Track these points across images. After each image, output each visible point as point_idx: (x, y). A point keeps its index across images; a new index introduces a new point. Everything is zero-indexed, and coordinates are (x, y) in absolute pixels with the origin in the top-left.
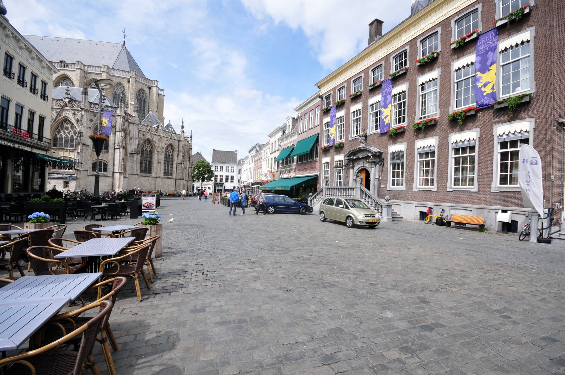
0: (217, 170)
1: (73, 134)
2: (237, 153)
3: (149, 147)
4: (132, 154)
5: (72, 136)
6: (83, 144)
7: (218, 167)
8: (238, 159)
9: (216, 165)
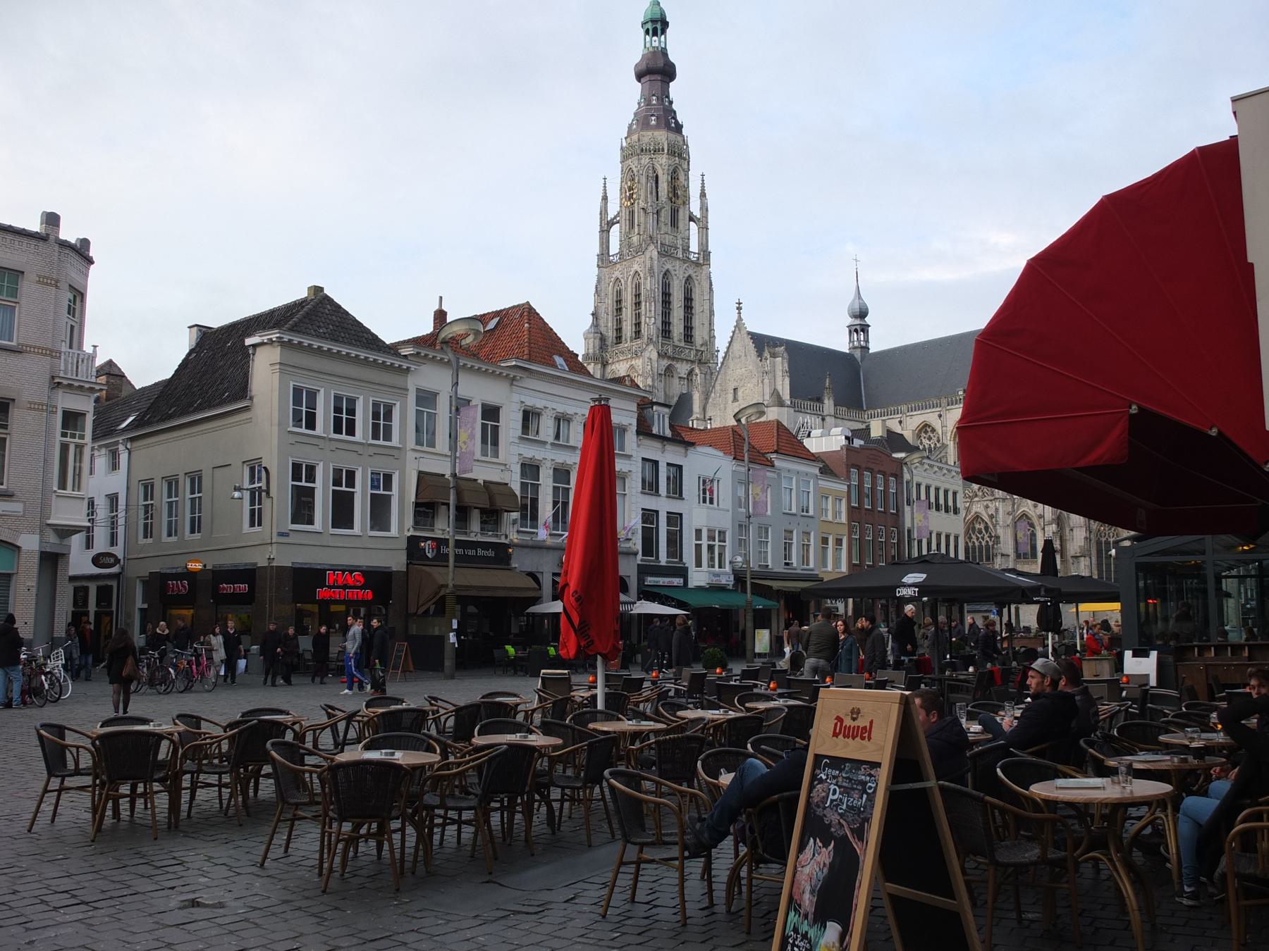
1: (988, 539)
3: (1111, 535)
4: (1077, 557)
5: (987, 542)
6: (1002, 555)
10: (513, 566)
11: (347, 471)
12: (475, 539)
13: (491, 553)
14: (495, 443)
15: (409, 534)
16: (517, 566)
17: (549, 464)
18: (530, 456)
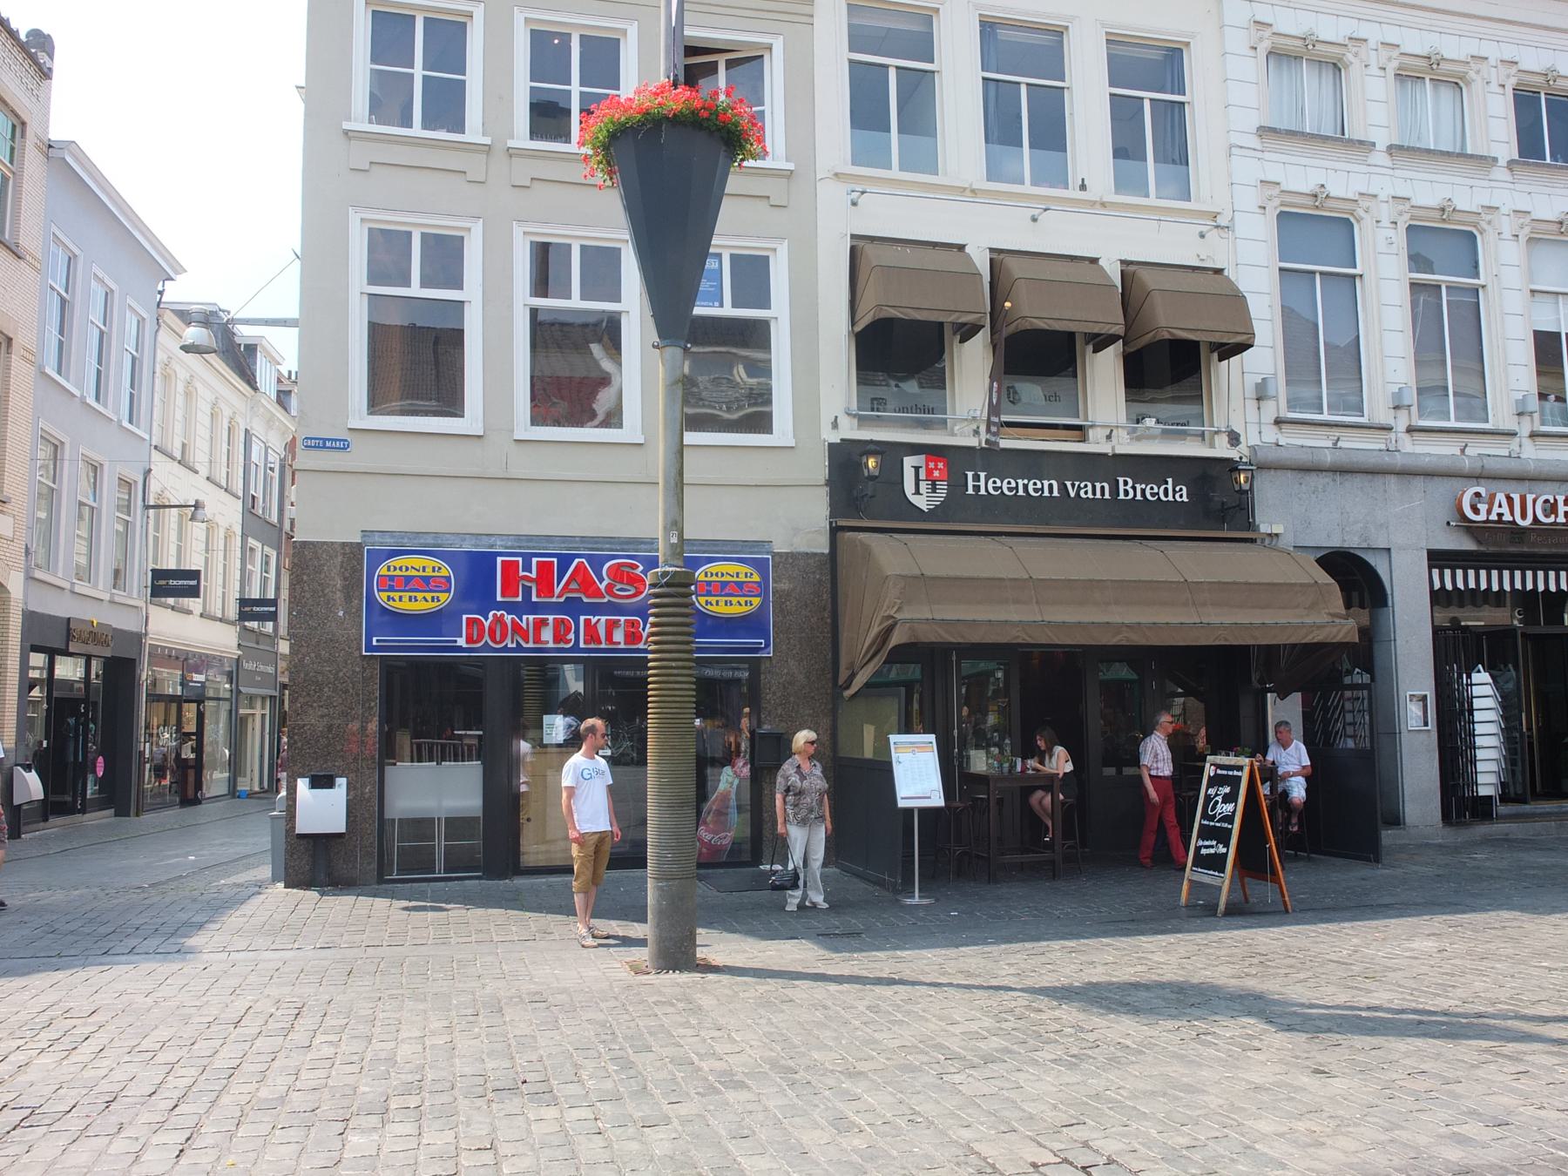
10: (1264, 528)
11: (583, 248)
12: (1105, 448)
13: (1176, 492)
14: (1176, 152)
15: (835, 438)
16: (1277, 529)
17: (1385, 212)
18: (1307, 186)
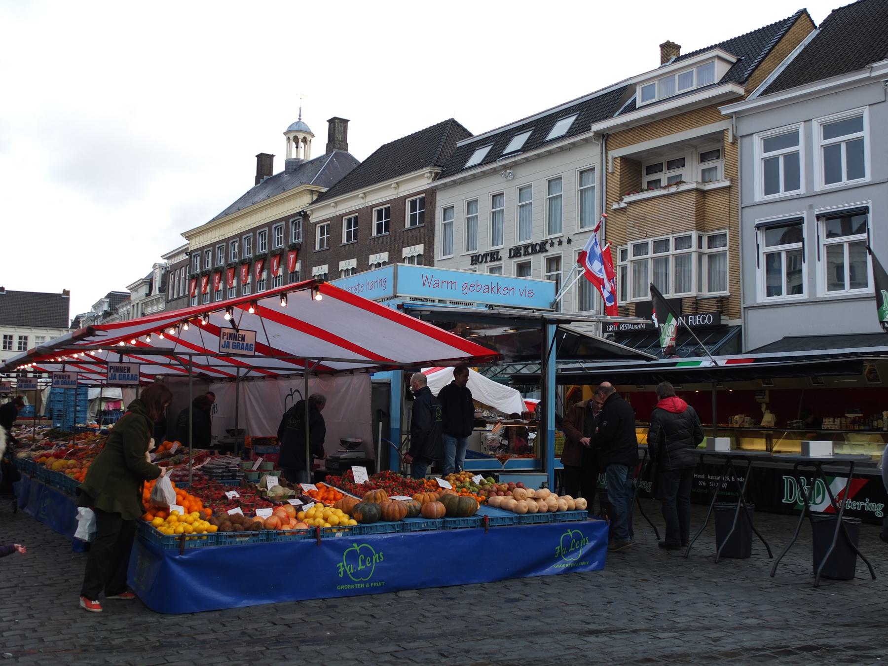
0: (10, 348)
2: (68, 300)
7: (11, 337)
8: (72, 316)
9: (6, 333)
